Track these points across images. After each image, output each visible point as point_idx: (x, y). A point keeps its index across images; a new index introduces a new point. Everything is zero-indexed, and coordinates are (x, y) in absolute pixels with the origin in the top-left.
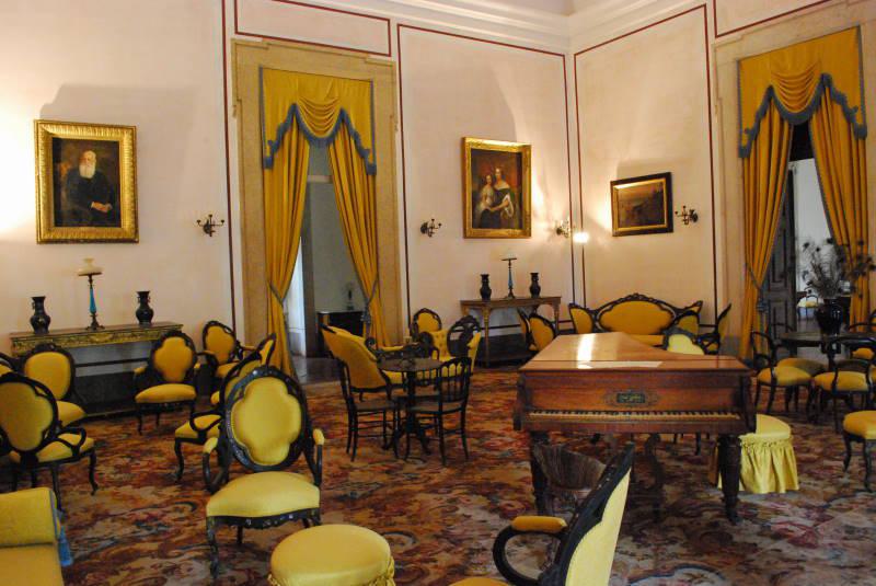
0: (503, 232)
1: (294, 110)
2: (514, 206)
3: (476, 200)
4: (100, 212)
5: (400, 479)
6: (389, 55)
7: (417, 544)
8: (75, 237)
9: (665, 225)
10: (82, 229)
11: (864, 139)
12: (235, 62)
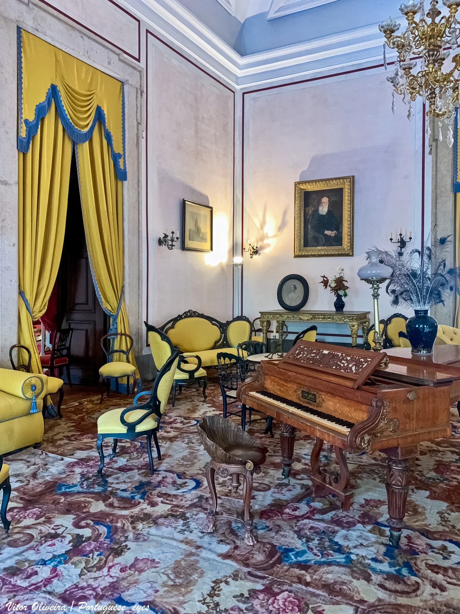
8: (313, 253)
10: (319, 248)
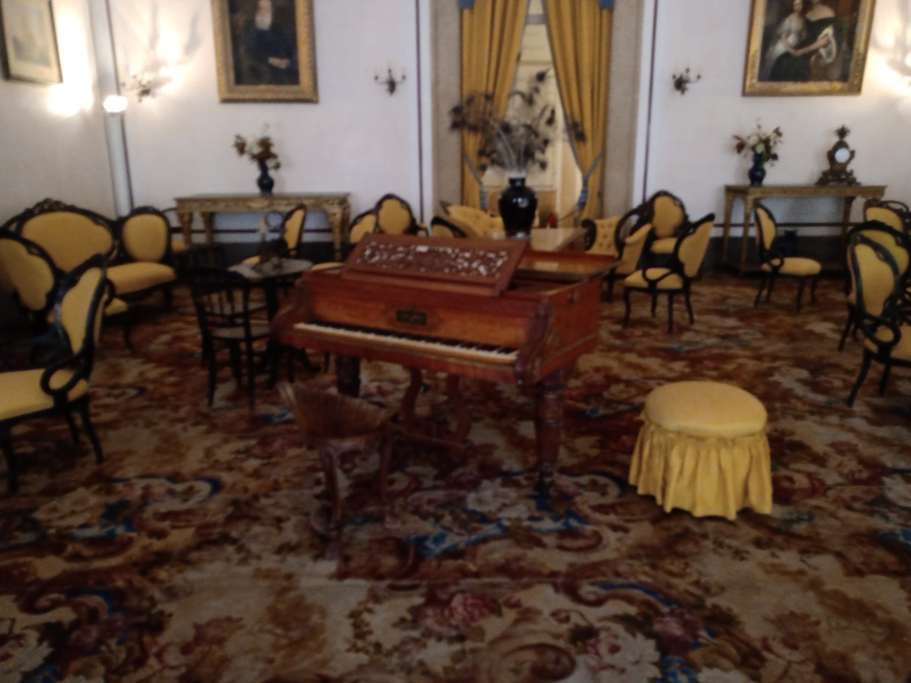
0: (811, 86)
2: (839, 45)
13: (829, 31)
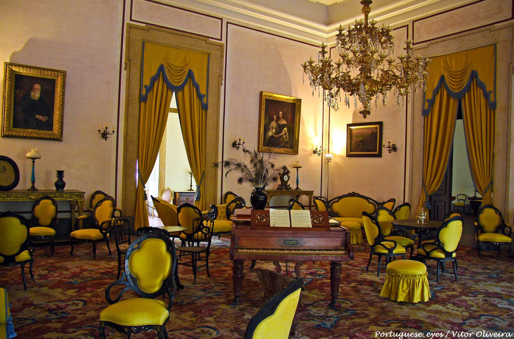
1: (161, 68)
2: (289, 135)
3: (266, 129)
4: (41, 121)
5: (210, 295)
6: (221, 40)
7: (219, 335)
9: (377, 153)
11: (494, 110)
12: (128, 38)
13: (286, 129)
